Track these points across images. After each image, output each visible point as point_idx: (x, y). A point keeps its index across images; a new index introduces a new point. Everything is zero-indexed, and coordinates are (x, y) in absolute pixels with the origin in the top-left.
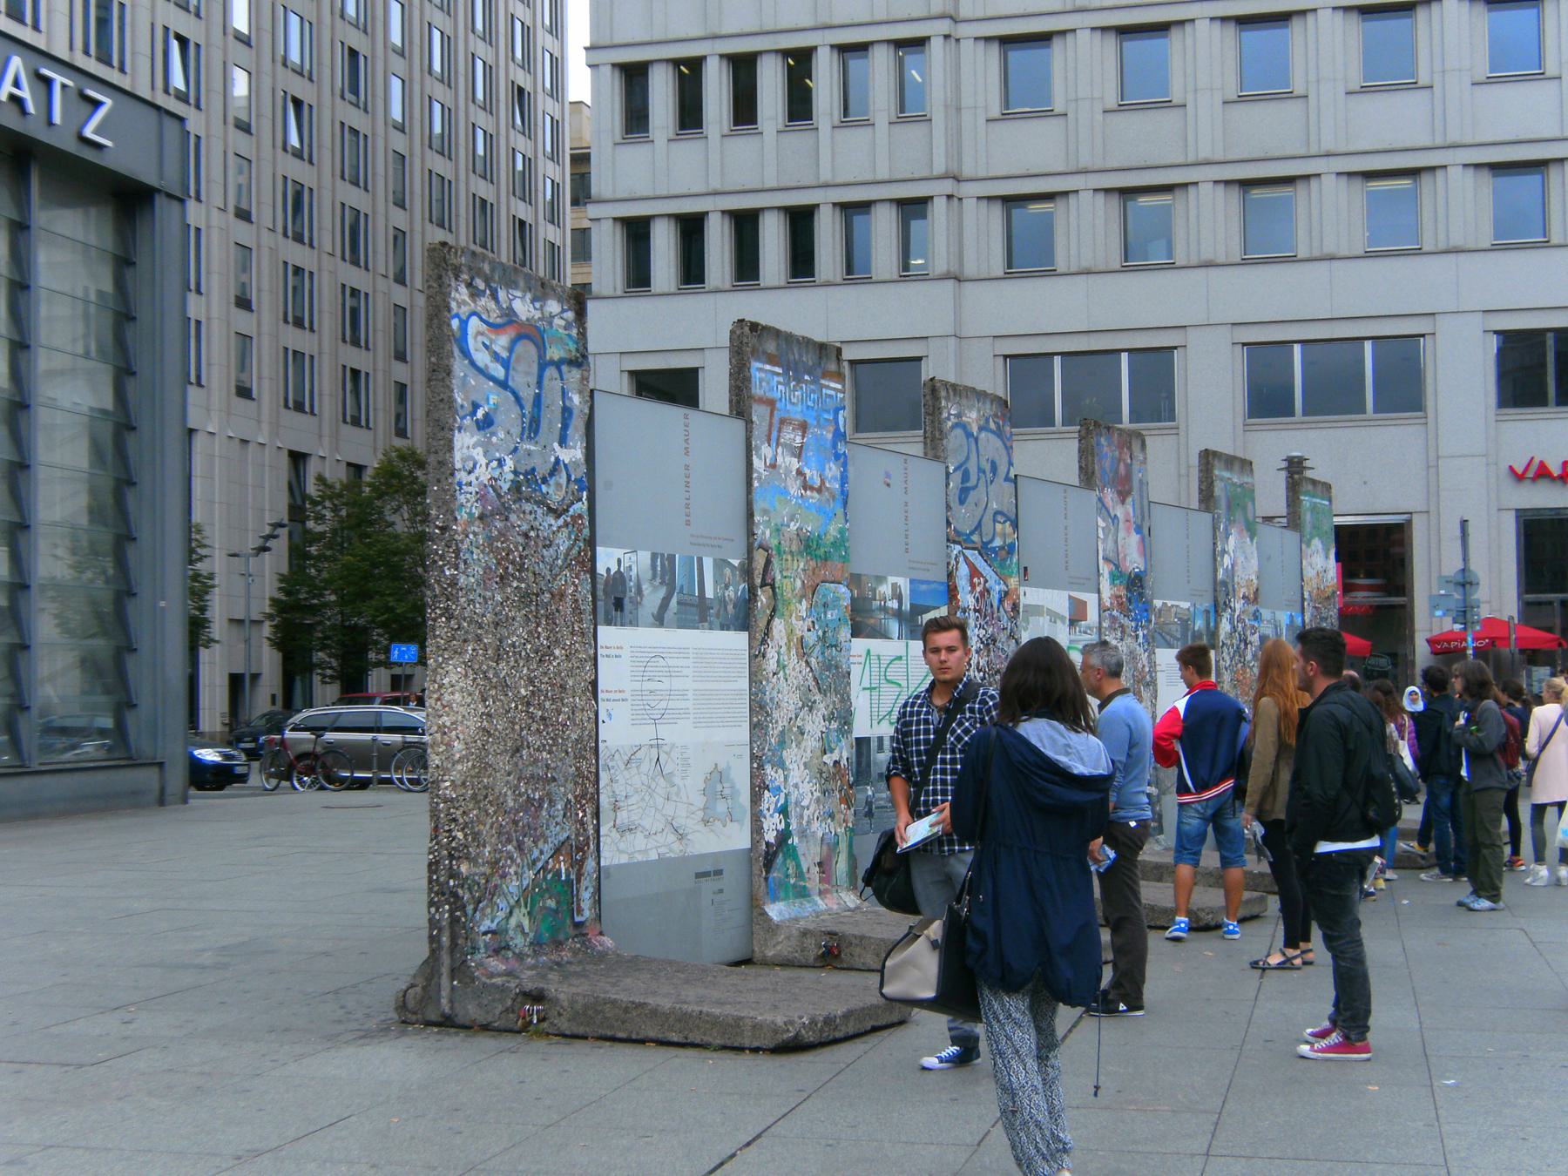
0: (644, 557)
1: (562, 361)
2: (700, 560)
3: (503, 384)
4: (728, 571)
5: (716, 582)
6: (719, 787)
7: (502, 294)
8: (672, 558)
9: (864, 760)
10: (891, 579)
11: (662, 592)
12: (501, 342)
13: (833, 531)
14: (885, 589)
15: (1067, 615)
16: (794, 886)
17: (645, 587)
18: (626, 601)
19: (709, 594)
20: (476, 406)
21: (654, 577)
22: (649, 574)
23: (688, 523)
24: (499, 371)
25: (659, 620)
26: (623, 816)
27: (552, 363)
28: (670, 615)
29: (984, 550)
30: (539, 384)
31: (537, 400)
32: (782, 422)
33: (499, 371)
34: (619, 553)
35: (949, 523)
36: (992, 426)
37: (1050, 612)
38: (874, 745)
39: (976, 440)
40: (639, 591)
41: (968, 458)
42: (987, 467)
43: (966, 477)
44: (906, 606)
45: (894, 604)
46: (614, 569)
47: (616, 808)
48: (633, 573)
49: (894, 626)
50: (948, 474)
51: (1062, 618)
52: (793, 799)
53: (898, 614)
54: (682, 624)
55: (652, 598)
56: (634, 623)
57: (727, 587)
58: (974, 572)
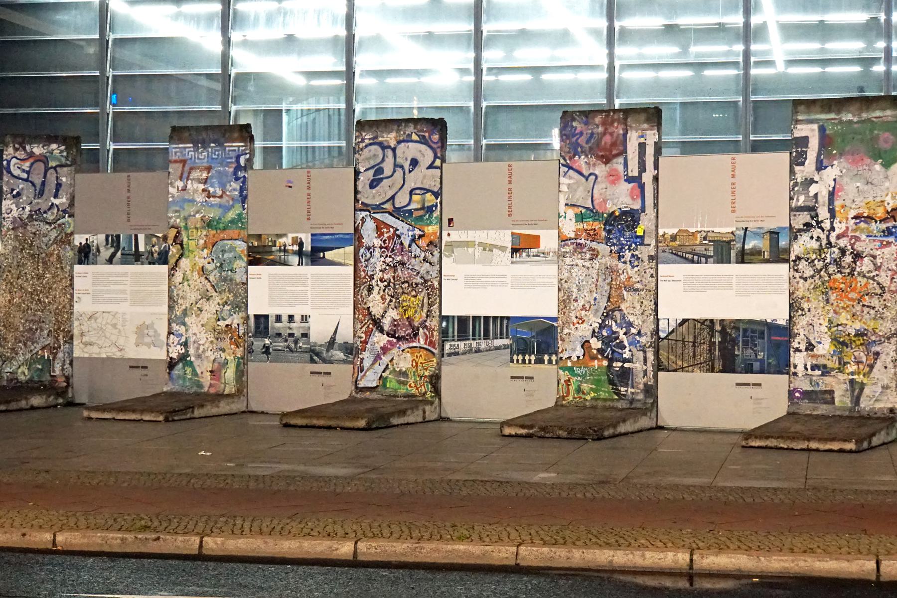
0: (102, 237)
1: (57, 166)
2: (136, 236)
3: (26, 180)
4: (154, 240)
5: (146, 244)
6: (146, 331)
7: (28, 147)
8: (118, 237)
9: (262, 326)
10: (290, 236)
11: (112, 250)
12: (26, 166)
13: (231, 215)
14: (287, 240)
15: (510, 246)
16: (190, 379)
17: (102, 249)
18: (91, 255)
19: (142, 248)
20: (13, 190)
21: (107, 244)
22: (104, 243)
23: (129, 221)
24: (25, 176)
25: (110, 261)
26: (85, 339)
27: (52, 168)
28: (115, 260)
29: (397, 213)
30: (45, 177)
31: (43, 184)
32: (191, 169)
33: (25, 176)
34: (87, 236)
35: (356, 200)
36: (415, 137)
37: (480, 244)
38: (272, 319)
39: (394, 150)
40: (98, 250)
41: (383, 160)
42: (407, 165)
43: (380, 171)
44: (307, 247)
45: (296, 248)
46: (84, 242)
47: (82, 335)
48: (95, 244)
49: (295, 259)
50: (357, 173)
51: (502, 249)
52: (192, 340)
53: (300, 253)
54: (124, 262)
55: (106, 253)
56: (95, 263)
57: (153, 246)
58: (380, 226)
